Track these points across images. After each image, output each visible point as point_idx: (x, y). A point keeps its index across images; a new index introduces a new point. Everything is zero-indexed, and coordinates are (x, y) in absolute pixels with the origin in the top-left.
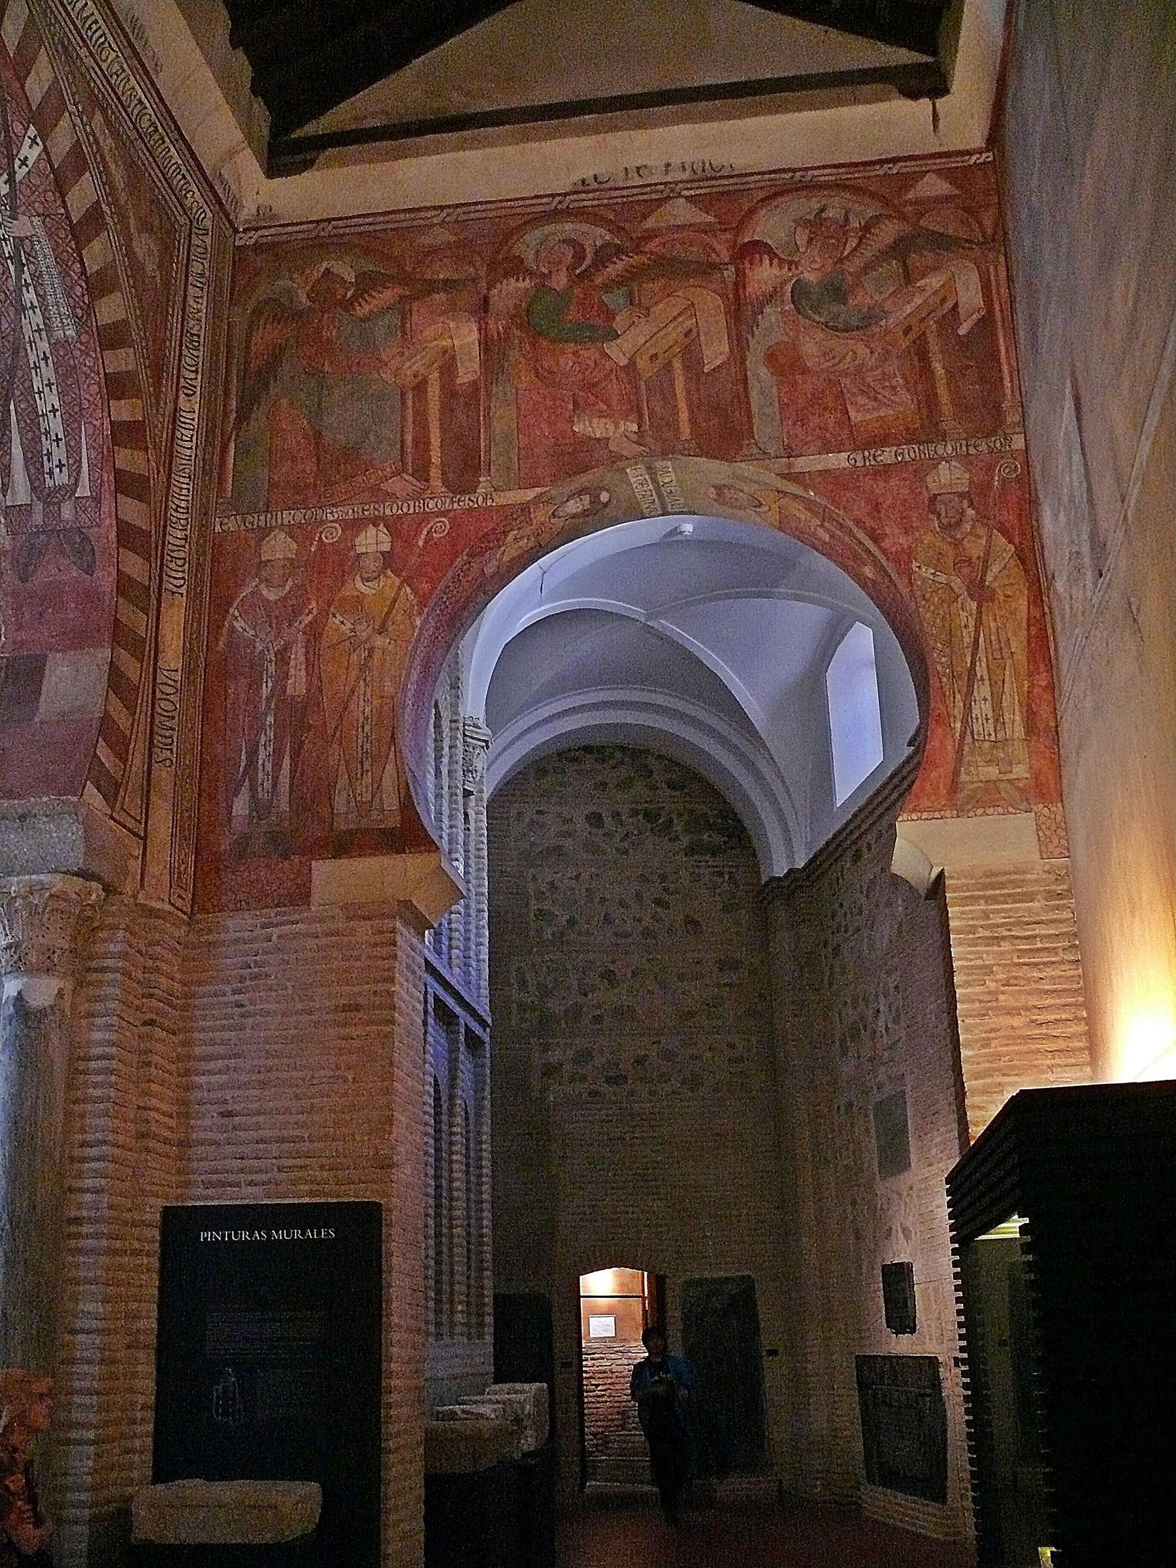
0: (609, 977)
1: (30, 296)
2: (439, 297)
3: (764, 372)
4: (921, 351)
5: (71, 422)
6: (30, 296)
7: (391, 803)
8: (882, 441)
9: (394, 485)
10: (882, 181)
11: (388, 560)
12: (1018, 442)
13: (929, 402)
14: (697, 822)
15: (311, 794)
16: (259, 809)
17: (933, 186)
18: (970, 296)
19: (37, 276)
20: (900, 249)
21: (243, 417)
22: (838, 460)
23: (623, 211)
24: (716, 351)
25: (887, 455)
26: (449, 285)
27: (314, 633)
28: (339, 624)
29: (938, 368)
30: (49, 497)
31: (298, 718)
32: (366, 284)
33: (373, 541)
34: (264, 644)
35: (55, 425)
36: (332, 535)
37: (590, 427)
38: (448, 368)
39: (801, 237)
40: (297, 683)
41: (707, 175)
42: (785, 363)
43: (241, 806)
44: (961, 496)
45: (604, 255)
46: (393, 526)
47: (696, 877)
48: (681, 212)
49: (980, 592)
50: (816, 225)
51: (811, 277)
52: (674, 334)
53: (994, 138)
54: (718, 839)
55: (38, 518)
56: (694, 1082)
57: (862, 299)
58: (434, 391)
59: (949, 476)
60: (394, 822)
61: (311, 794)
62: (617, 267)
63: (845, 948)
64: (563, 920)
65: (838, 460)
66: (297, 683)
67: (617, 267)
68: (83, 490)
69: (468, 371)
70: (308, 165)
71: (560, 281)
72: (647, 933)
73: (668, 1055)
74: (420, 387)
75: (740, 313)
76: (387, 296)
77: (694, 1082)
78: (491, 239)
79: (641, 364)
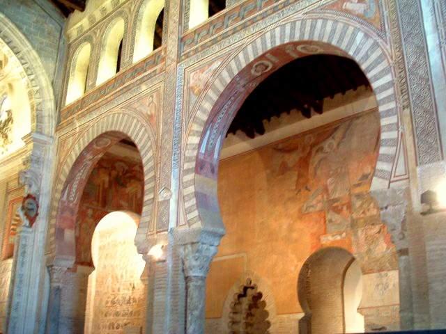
1: (82, 171)
5: (77, 189)
6: (82, 171)
24: (139, 196)
26: (105, 168)
30: (69, 201)
33: (90, 212)
35: (74, 191)
36: (84, 208)
38: (104, 184)
46: (94, 209)
58: (101, 189)
62: (128, 175)
68: (75, 202)
69: (106, 186)
71: (121, 174)
74: (99, 186)
79: (130, 196)
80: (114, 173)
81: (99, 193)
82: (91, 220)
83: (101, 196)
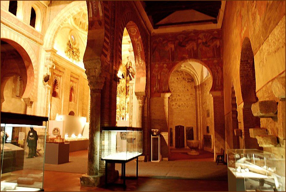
0: (179, 95)
1: (138, 48)
2: (170, 42)
3: (200, 51)
4: (214, 49)
6: (138, 48)
7: (167, 88)
8: (210, 57)
9: (167, 60)
10: (211, 32)
11: (167, 67)
12: (222, 58)
13: (214, 54)
14: (188, 79)
15: (161, 88)
16: (156, 89)
17: (216, 32)
18: (218, 44)
19: (139, 46)
20: (212, 39)
21: (153, 53)
22: (206, 59)
23: (186, 33)
24: (195, 48)
25: (210, 59)
26: (171, 41)
27: (160, 74)
28: (162, 73)
29: (215, 50)
31: (159, 81)
32: (164, 40)
33: (165, 65)
34: (156, 74)
36: (161, 65)
37: (184, 55)
38: (171, 49)
39: (203, 37)
40: (159, 78)
41: (195, 30)
42: (201, 50)
43: (155, 89)
44: (216, 63)
45: (185, 38)
47: (188, 85)
48: (192, 34)
49: (218, 72)
50: (205, 36)
51: (204, 41)
52: (192, 47)
53: (221, 28)
54: (191, 81)
55: (139, 65)
56: (187, 107)
57: (208, 44)
59: (215, 61)
60: (168, 90)
61: (161, 88)
63: (204, 94)
64: (174, 89)
65: (206, 59)
66: (159, 78)
67: (186, 40)
69: (173, 49)
70: (157, 28)
72: (183, 91)
73: (185, 104)
74: (169, 51)
75: (198, 45)
76: (165, 42)
77: (187, 107)
78: (174, 36)
79: (189, 50)
80: (177, 42)
81: (169, 55)
82: (166, 70)
83: (170, 56)
